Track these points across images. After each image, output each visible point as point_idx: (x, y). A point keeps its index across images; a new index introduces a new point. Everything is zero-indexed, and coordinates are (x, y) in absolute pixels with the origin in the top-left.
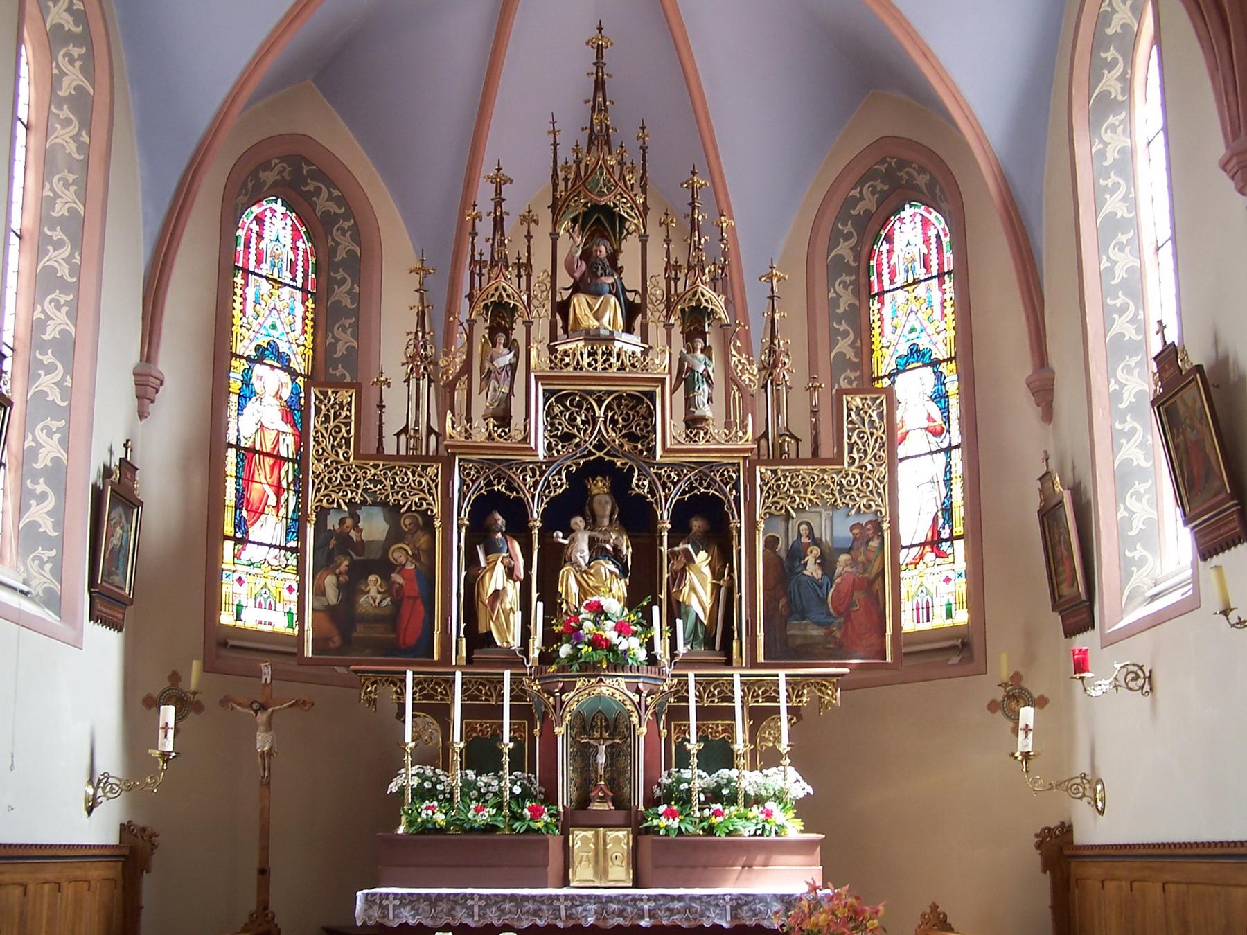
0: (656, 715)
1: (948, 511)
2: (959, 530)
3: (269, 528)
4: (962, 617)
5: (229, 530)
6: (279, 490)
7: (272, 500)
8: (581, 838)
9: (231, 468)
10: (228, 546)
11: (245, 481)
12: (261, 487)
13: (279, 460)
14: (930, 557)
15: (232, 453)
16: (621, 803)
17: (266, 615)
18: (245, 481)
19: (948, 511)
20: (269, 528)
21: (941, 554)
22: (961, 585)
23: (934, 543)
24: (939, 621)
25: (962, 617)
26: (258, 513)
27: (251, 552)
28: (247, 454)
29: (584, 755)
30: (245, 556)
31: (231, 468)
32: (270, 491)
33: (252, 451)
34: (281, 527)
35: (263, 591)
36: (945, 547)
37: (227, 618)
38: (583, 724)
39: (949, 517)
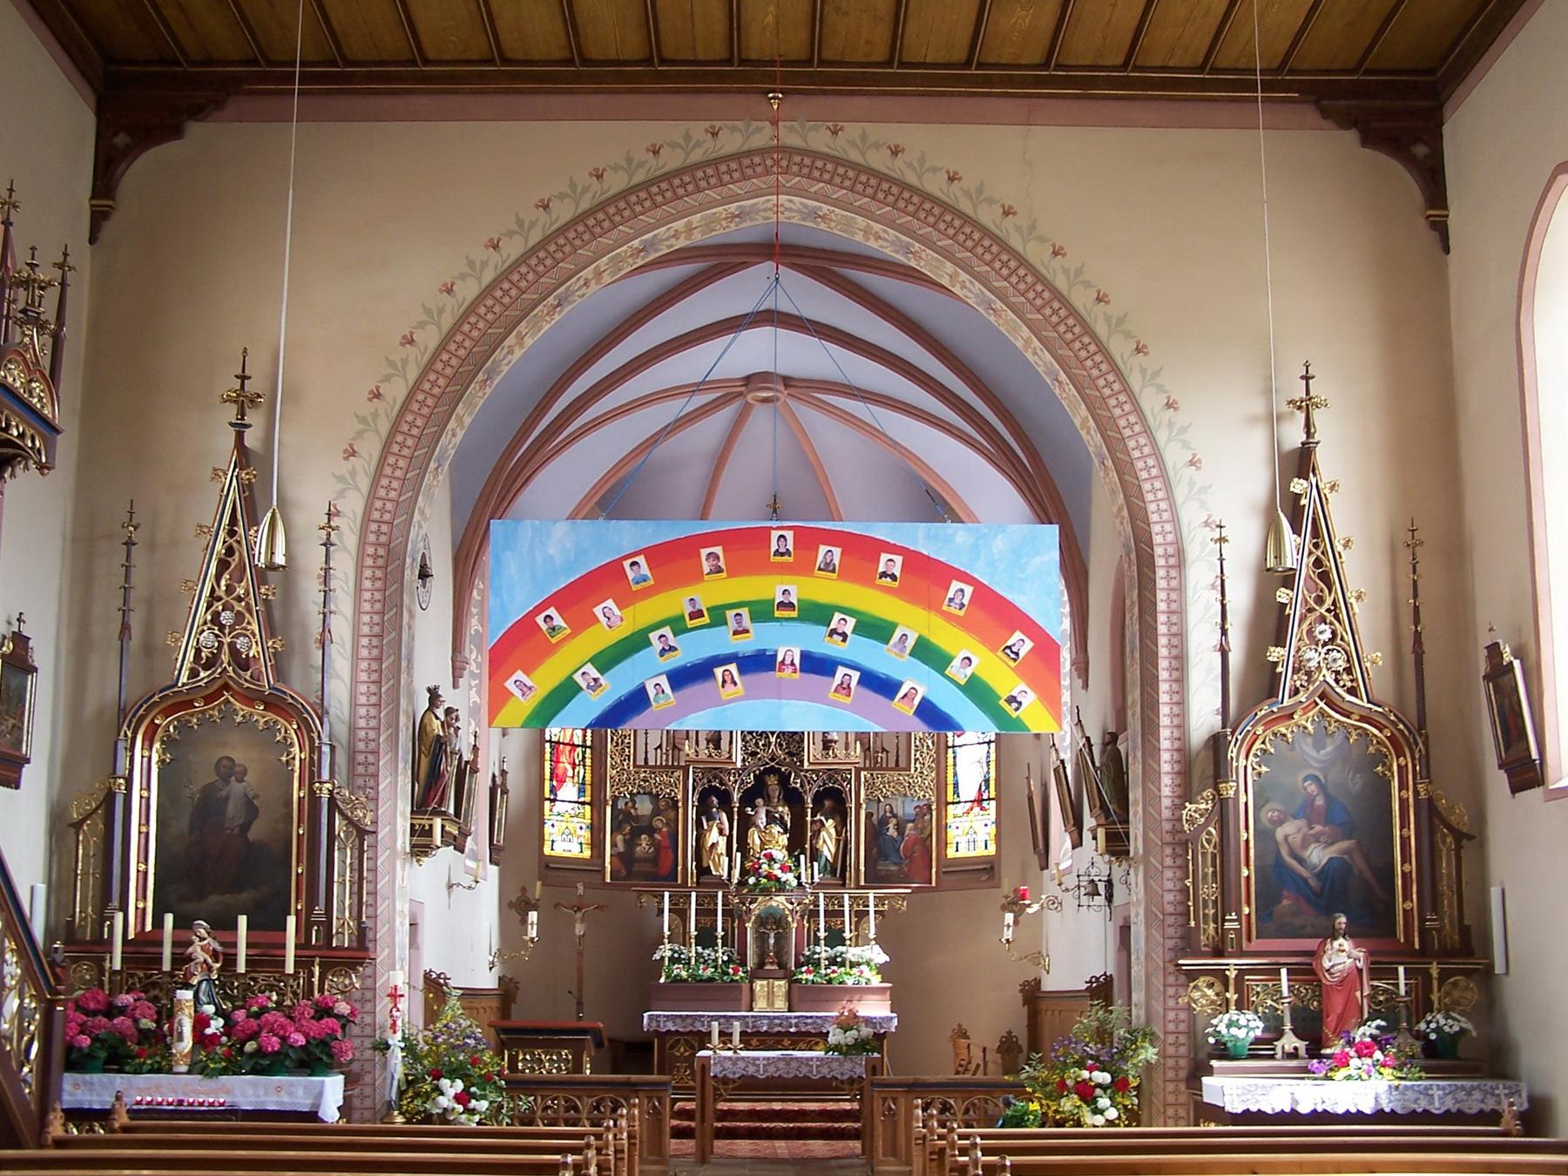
0: (802, 916)
1: (987, 781)
2: (993, 795)
3: (569, 791)
4: (992, 850)
5: (547, 794)
6: (574, 766)
7: (570, 773)
8: (759, 985)
9: (547, 756)
10: (547, 804)
11: (555, 761)
12: (565, 765)
13: (574, 746)
14: (977, 809)
15: (547, 745)
16: (782, 965)
17: (567, 846)
18: (555, 761)
19: (987, 781)
20: (569, 791)
21: (982, 809)
22: (992, 829)
23: (979, 801)
24: (980, 852)
25: (992, 850)
26: (562, 782)
27: (559, 807)
28: (555, 745)
29: (761, 939)
30: (555, 810)
31: (547, 756)
32: (569, 768)
33: (558, 743)
34: (575, 790)
35: (567, 834)
36: (985, 804)
37: (547, 851)
38: (762, 921)
39: (988, 787)
